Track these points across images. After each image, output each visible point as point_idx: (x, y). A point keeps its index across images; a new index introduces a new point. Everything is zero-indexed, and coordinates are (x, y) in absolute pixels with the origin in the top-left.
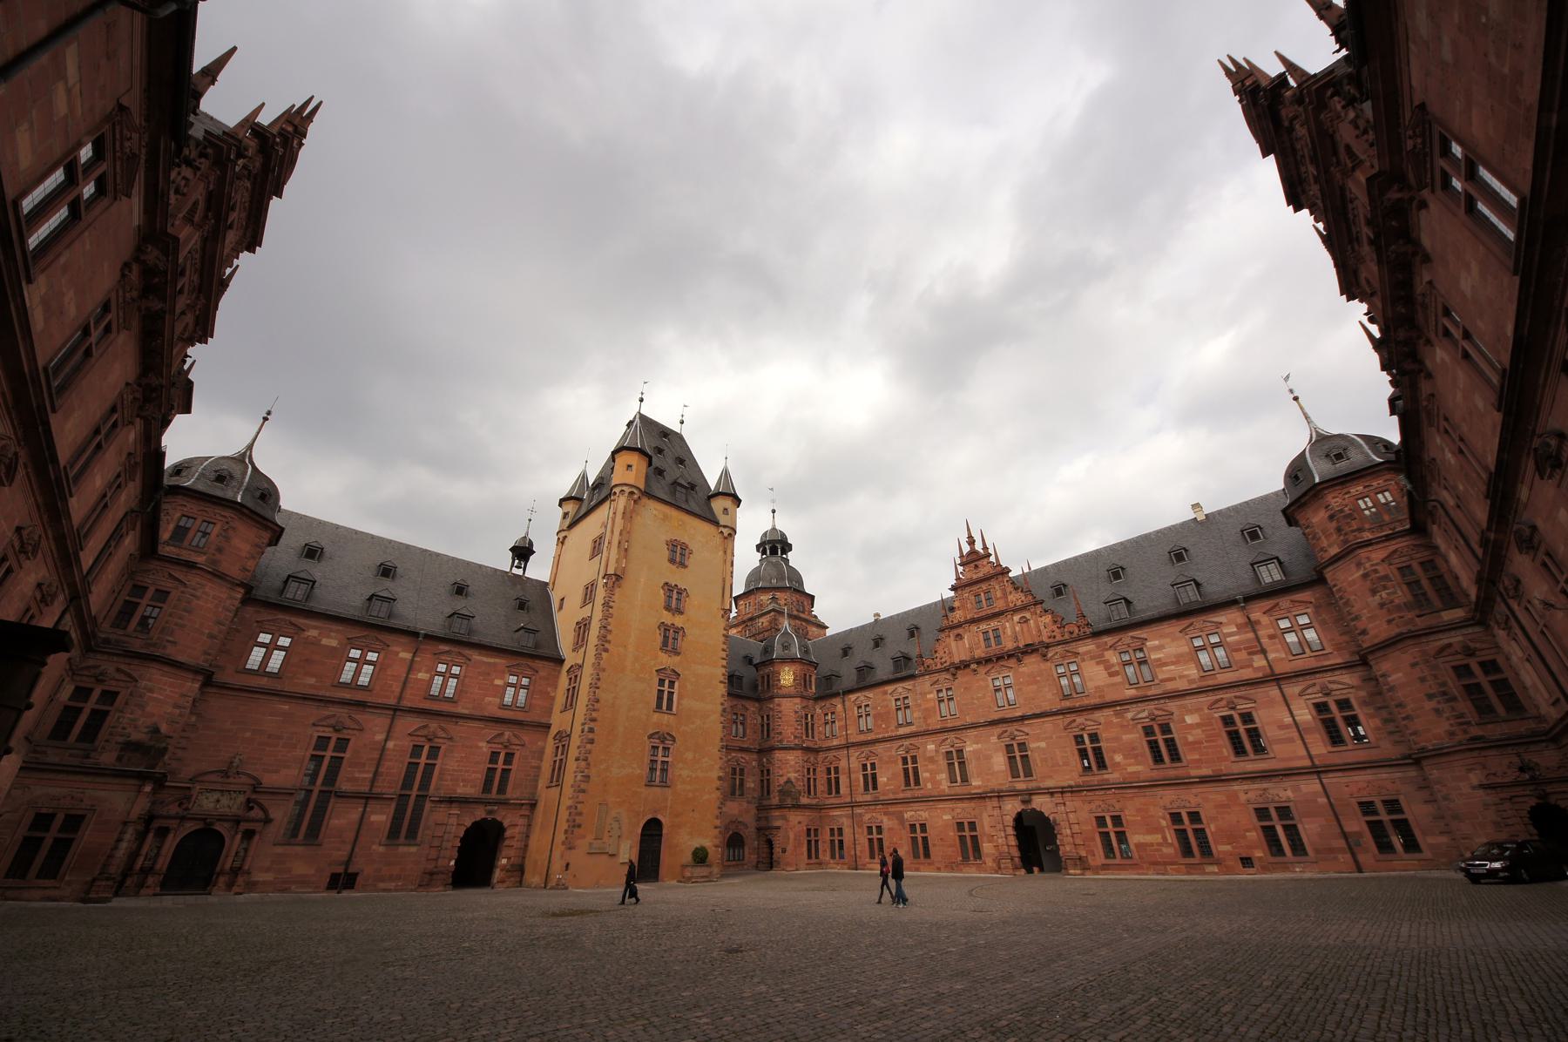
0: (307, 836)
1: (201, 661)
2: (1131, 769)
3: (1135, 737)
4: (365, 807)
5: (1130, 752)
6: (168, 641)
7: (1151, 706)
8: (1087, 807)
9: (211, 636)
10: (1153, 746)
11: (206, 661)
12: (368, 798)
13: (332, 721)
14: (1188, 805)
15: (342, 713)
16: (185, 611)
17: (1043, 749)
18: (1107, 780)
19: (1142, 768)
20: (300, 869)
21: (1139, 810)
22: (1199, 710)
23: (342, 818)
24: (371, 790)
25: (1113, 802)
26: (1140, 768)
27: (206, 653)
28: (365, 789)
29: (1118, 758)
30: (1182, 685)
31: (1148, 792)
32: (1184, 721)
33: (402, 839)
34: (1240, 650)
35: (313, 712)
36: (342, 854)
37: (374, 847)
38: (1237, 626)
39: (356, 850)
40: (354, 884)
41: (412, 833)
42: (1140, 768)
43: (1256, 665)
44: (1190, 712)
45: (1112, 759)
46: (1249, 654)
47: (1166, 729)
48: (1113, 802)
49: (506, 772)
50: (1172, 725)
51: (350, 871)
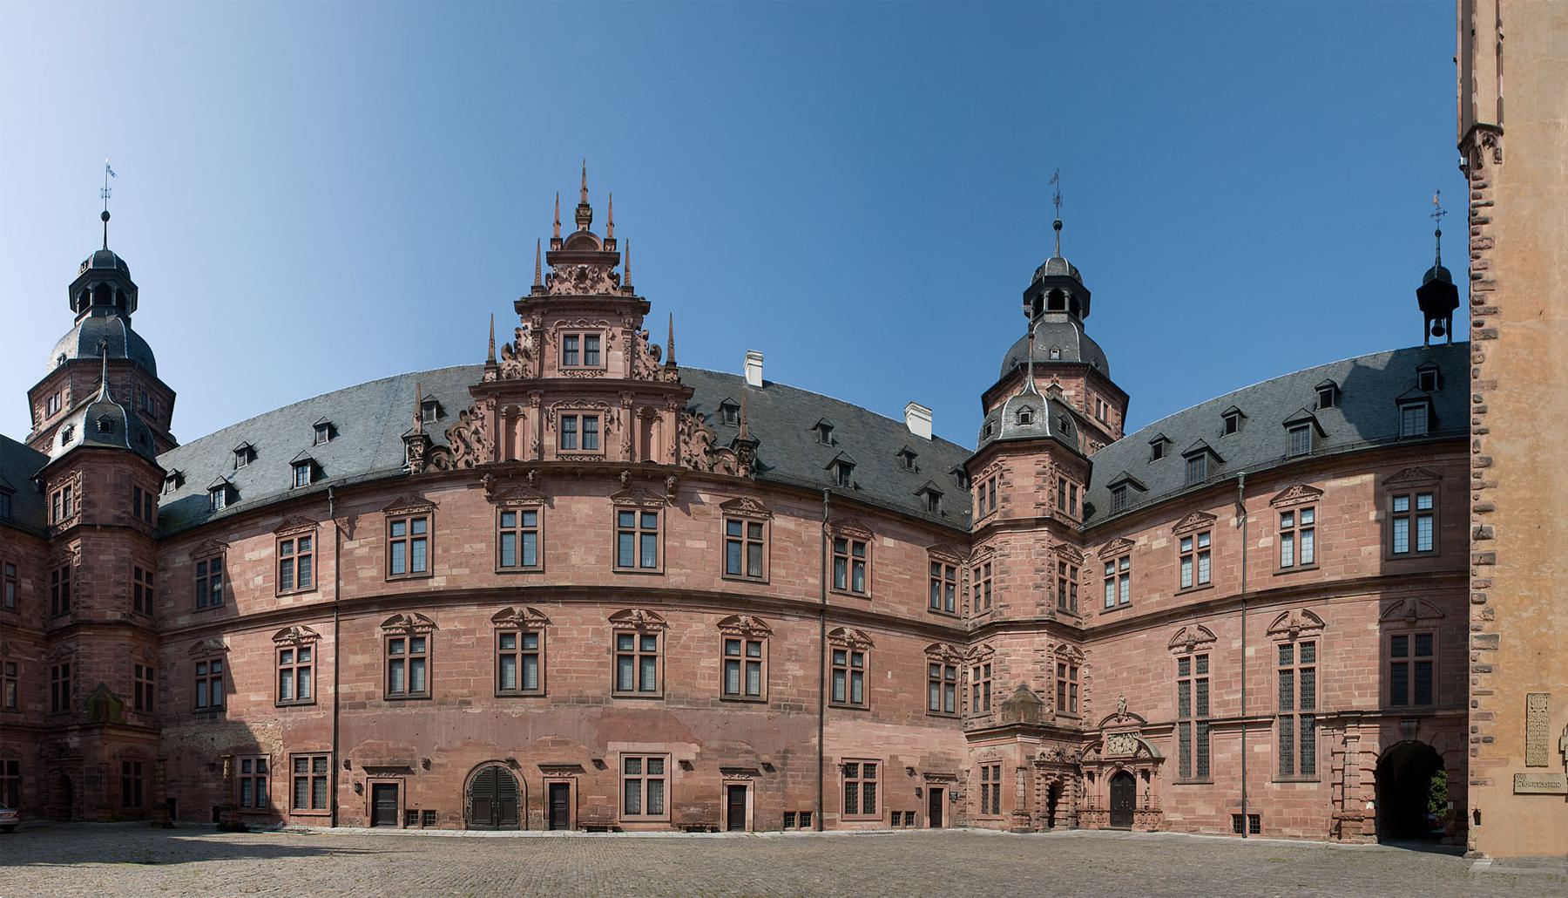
0: (1199, 774)
1: (1038, 614)
4: (1244, 737)
6: (1001, 606)
9: (1037, 587)
11: (1042, 612)
12: (1244, 724)
13: (1184, 638)
15: (1191, 626)
16: (1001, 573)
20: (1203, 809)
23: (1225, 749)
24: (1243, 715)
27: (1038, 605)
28: (1239, 713)
33: (1297, 774)
35: (1168, 631)
36: (1235, 793)
37: (1266, 784)
39: (1248, 788)
40: (1259, 827)
41: (1309, 768)
49: (1424, 669)
51: (1248, 812)
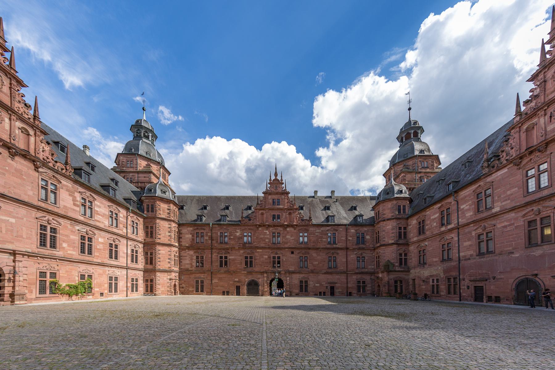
2: (69, 252)
3: (76, 238)
5: (71, 244)
7: (88, 228)
8: (37, 266)
10: (83, 245)
14: (116, 274)
17: (11, 223)
18: (55, 254)
19: (75, 253)
21: (67, 271)
22: (104, 238)
25: (55, 266)
26: (74, 253)
29: (65, 245)
30: (102, 226)
31: (75, 264)
32: (98, 240)
34: (121, 224)
38: (123, 215)
42: (74, 253)
43: (124, 231)
44: (101, 237)
45: (61, 244)
46: (123, 226)
47: (90, 240)
48: (55, 266)
50: (93, 239)
